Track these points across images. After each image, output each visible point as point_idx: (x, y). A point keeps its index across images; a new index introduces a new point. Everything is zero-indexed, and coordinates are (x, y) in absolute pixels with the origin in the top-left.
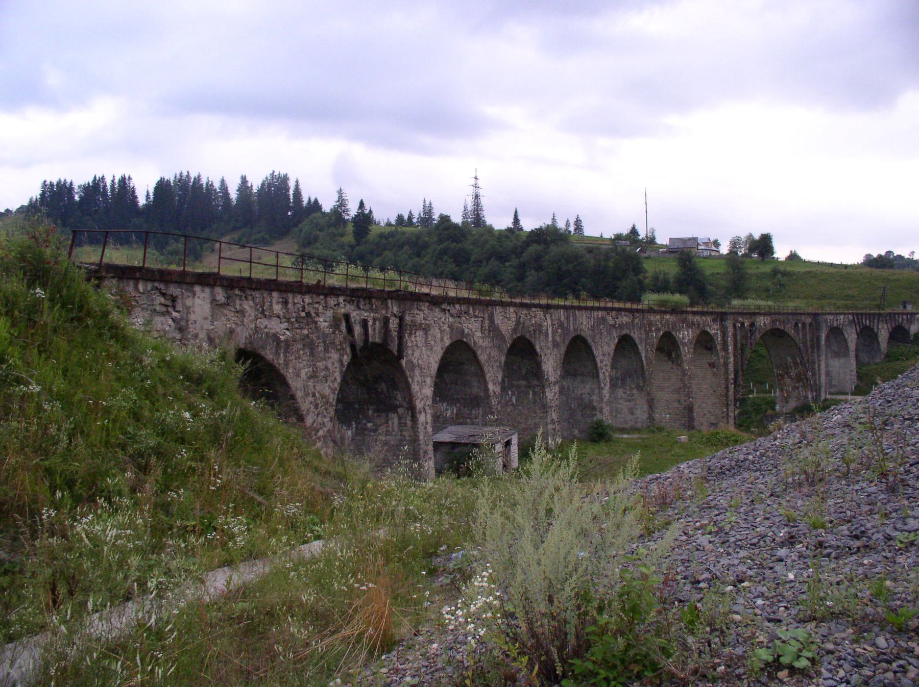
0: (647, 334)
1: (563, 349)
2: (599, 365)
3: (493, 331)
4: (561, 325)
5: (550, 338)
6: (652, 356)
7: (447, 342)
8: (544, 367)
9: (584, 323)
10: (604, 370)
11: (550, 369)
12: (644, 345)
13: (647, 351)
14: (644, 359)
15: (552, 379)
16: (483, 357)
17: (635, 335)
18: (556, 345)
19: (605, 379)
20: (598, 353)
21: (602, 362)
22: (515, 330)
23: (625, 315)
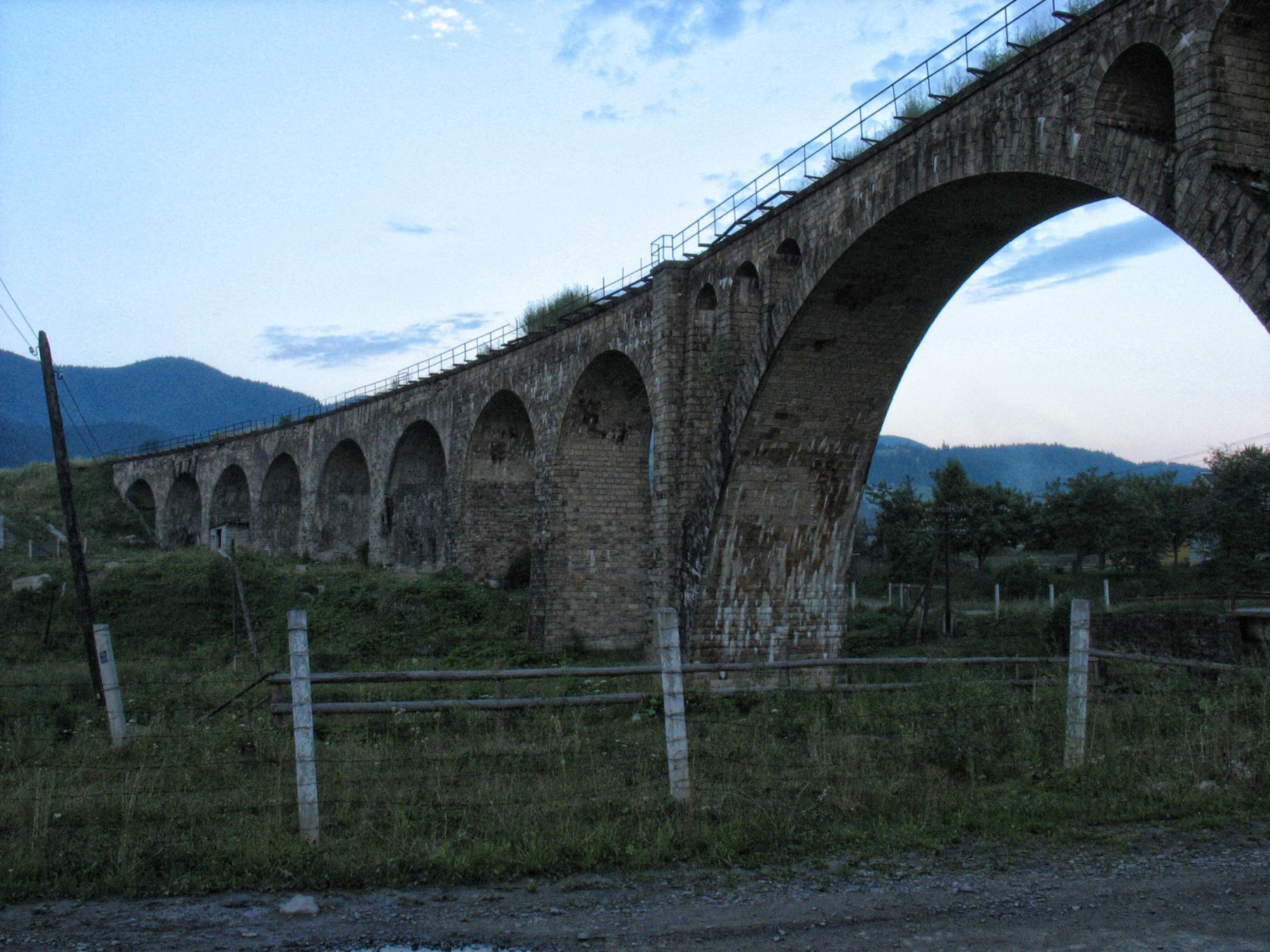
0: (457, 408)
1: (324, 457)
2: (370, 469)
3: (259, 453)
4: (325, 431)
5: (311, 448)
6: (463, 446)
7: (225, 466)
8: (302, 478)
9: (355, 422)
10: (376, 476)
11: (308, 479)
12: (448, 431)
13: (455, 438)
14: (447, 452)
15: (309, 488)
16: (248, 473)
17: (434, 417)
18: (315, 454)
19: (377, 487)
20: (370, 456)
21: (374, 465)
22: (276, 450)
23: (420, 392)
